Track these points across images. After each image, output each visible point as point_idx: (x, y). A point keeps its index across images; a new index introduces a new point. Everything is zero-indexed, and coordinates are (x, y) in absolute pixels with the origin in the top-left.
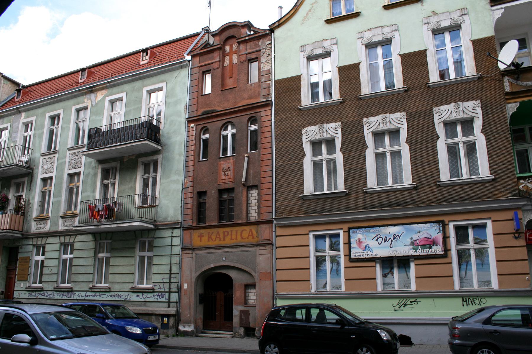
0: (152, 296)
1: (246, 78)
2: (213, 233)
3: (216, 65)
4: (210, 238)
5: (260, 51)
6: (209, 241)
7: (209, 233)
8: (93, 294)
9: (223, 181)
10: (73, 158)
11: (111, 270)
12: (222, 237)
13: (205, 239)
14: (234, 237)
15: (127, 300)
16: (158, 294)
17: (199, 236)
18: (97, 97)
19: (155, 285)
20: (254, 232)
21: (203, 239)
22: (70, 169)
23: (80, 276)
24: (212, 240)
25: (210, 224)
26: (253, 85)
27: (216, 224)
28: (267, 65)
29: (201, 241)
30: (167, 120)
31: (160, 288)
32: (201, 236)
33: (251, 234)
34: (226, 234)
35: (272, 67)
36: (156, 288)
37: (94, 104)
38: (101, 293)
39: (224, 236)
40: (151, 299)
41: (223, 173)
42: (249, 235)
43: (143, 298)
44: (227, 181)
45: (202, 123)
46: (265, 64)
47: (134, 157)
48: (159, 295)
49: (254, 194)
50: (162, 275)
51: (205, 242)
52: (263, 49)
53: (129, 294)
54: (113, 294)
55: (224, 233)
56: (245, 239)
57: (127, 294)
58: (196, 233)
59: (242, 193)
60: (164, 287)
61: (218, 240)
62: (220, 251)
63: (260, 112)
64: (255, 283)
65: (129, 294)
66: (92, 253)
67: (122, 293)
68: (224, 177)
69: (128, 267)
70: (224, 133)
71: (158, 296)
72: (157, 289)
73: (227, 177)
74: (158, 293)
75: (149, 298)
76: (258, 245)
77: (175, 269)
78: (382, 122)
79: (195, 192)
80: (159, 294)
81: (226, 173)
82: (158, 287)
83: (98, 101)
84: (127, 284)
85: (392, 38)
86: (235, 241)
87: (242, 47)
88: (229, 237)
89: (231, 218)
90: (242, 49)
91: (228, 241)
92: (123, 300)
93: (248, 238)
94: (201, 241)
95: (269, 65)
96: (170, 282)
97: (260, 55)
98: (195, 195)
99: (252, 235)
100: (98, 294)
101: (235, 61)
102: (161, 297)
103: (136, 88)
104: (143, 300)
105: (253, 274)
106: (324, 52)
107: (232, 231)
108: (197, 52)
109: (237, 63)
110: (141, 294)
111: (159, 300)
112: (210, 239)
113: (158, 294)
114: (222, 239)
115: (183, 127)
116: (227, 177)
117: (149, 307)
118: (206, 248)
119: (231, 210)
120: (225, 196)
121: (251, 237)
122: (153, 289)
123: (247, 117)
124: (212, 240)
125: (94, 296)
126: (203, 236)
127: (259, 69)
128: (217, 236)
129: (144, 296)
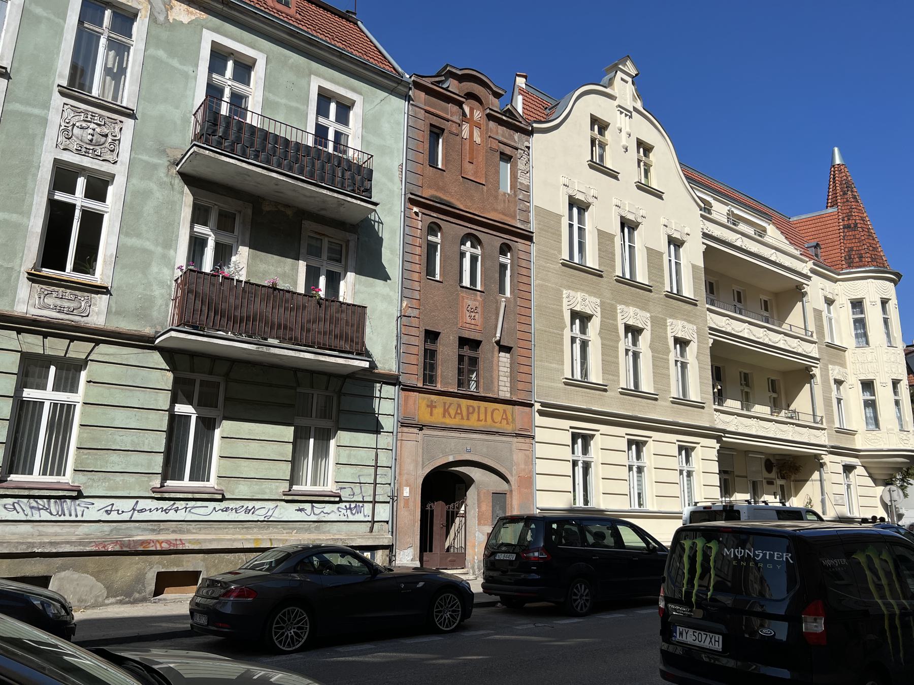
0: (336, 510)
2: (451, 404)
4: (446, 411)
5: (517, 149)
6: (444, 416)
7: (445, 403)
8: (166, 504)
9: (468, 325)
10: (84, 124)
12: (465, 413)
13: (438, 411)
14: (482, 417)
15: (270, 519)
16: (348, 507)
17: (428, 406)
19: (341, 488)
21: (435, 411)
22: (64, 149)
23: (114, 457)
24: (450, 416)
25: (445, 389)
29: (431, 415)
31: (353, 495)
32: (431, 406)
33: (504, 417)
36: (345, 495)
39: (468, 414)
40: (332, 517)
42: (502, 419)
44: (473, 327)
47: (289, 212)
48: (350, 508)
51: (437, 417)
53: (277, 506)
54: (232, 505)
56: (496, 423)
57: (271, 505)
59: (493, 352)
60: (361, 492)
62: (463, 435)
65: (277, 506)
67: (258, 505)
69: (275, 446)
71: (349, 511)
72: (347, 496)
74: (348, 505)
75: (328, 514)
76: (518, 435)
77: (384, 459)
80: (350, 505)
81: (473, 314)
83: (174, 19)
84: (274, 484)
86: (483, 423)
87: (492, 124)
88: (475, 415)
91: (473, 423)
93: (501, 423)
94: (431, 415)
96: (375, 484)
99: (506, 419)
100: (181, 505)
102: (354, 512)
104: (314, 518)
105: (509, 477)
107: (479, 407)
108: (427, 82)
110: (307, 506)
111: (351, 518)
112: (447, 413)
113: (348, 507)
114: (465, 417)
117: (329, 532)
121: (504, 422)
124: (450, 416)
125: (166, 511)
126: (435, 407)
128: (457, 410)
129: (317, 511)
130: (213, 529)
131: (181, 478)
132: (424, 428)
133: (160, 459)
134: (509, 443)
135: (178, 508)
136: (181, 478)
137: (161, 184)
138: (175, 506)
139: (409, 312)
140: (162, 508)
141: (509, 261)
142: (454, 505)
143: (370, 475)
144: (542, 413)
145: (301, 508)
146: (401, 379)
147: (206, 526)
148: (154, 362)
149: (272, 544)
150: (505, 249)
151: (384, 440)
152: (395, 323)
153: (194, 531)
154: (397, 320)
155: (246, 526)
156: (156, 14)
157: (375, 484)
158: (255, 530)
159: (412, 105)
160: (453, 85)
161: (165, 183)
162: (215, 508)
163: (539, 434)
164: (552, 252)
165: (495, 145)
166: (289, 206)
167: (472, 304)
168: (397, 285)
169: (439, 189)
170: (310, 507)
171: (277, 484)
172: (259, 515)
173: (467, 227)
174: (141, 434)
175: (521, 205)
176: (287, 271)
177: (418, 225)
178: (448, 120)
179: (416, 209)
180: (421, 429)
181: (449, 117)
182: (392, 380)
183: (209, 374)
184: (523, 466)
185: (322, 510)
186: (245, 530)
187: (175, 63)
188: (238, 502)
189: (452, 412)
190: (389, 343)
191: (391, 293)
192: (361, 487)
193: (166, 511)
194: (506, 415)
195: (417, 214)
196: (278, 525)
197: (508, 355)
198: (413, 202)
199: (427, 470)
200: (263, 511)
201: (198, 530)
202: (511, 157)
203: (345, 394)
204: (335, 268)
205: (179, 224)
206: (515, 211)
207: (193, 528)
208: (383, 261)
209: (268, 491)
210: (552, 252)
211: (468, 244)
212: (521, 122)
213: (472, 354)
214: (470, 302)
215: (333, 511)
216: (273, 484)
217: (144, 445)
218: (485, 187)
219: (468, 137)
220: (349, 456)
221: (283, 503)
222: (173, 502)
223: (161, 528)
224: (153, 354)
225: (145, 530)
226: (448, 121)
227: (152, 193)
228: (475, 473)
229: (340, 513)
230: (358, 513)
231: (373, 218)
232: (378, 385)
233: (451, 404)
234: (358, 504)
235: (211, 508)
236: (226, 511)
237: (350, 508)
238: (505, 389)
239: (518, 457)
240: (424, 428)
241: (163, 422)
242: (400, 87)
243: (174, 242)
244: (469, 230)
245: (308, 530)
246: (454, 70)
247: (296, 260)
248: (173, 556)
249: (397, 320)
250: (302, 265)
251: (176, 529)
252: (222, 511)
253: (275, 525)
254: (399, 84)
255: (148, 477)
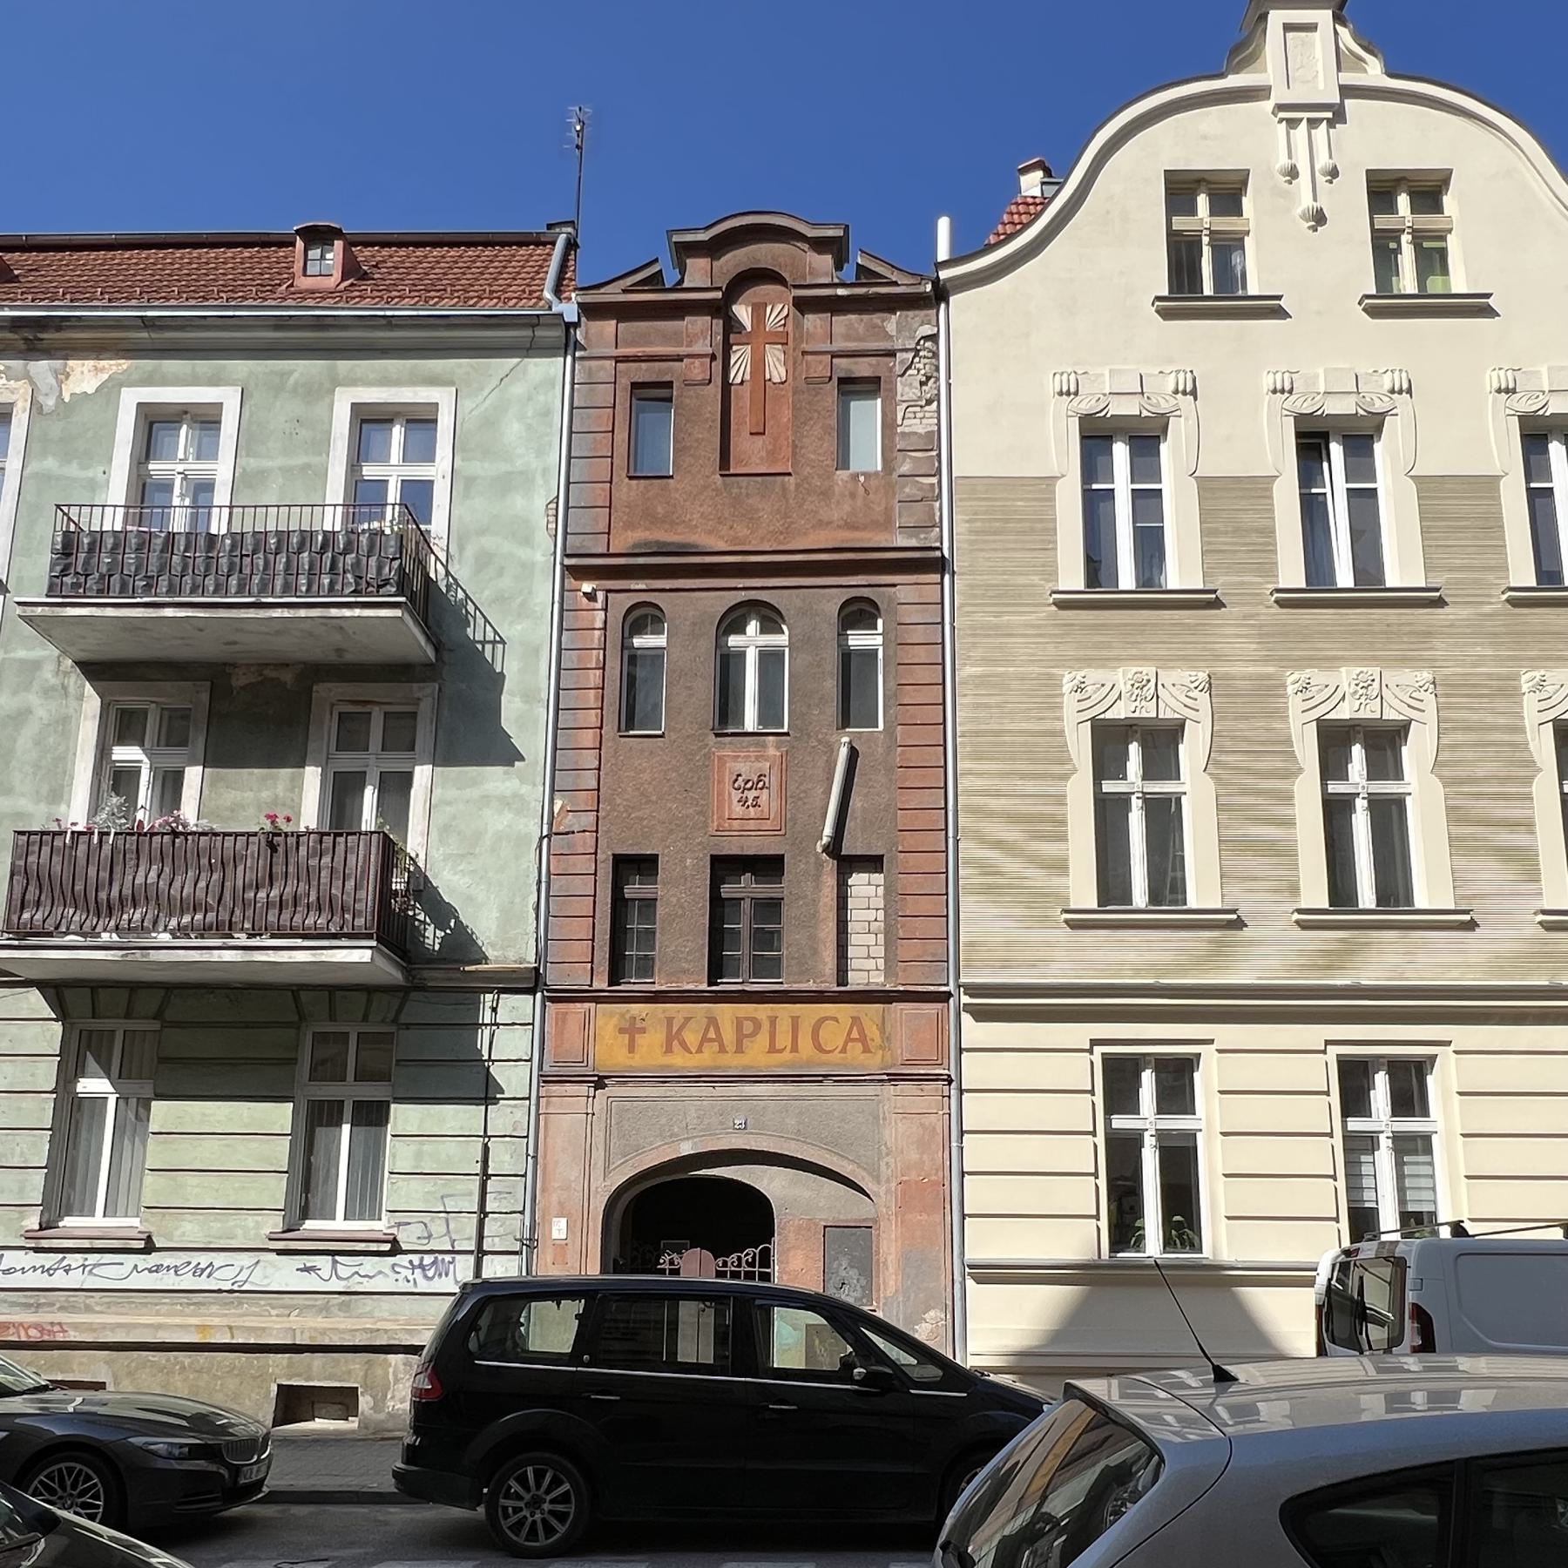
0: (387, 1271)
1: (831, 444)
2: (688, 1020)
3: (697, 370)
4: (673, 1039)
5: (891, 354)
6: (669, 1050)
7: (670, 1021)
8: (49, 1260)
11: (156, 1153)
12: (729, 1035)
13: (652, 1040)
14: (784, 1040)
15: (243, 1288)
16: (416, 1263)
18: (68, 376)
19: (399, 1224)
20: (873, 1032)
21: (641, 1040)
25: (673, 986)
26: (862, 479)
27: (704, 987)
28: (919, 415)
29: (632, 1048)
30: (461, 548)
31: (430, 1237)
33: (855, 1034)
34: (748, 1027)
35: (939, 425)
36: (407, 1239)
37: (50, 403)
38: (93, 1258)
39: (740, 1038)
41: (736, 795)
42: (849, 1039)
43: (338, 1278)
44: (752, 825)
45: (633, 587)
46: (910, 409)
47: (287, 677)
48: (421, 1266)
49: (863, 886)
50: (440, 1180)
51: (651, 1052)
52: (906, 350)
53: (258, 1262)
54: (167, 1259)
55: (739, 1023)
56: (829, 1052)
57: (246, 1259)
58: (608, 1017)
59: (817, 878)
60: (448, 1231)
61: (710, 1050)
62: (721, 1090)
63: (894, 585)
64: (875, 1221)
65: (258, 1262)
66: (46, 1074)
67: (219, 1259)
68: (738, 810)
69: (254, 1144)
70: (734, 641)
71: (418, 1271)
72: (416, 1240)
73: (752, 812)
74: (416, 1258)
75: (371, 1277)
76: (895, 1078)
77: (504, 1158)
78: (1356, 692)
79: (605, 856)
81: (751, 794)
82: (417, 1230)
84: (251, 1220)
85: (1383, 415)
87: (813, 321)
88: (763, 1039)
89: (771, 967)
90: (811, 330)
91: (757, 1056)
92: (228, 1287)
93: (844, 1051)
94: (632, 1048)
95: (927, 415)
96: (483, 1213)
97: (891, 370)
98: (606, 871)
99: (863, 1039)
100: (75, 1260)
101: (776, 369)
102: (430, 1274)
103: (292, 380)
106: (1145, 413)
107: (773, 1021)
108: (612, 294)
109: (783, 383)
110: (324, 1262)
111: (423, 1286)
113: (416, 1263)
115: (544, 591)
116: (752, 812)
117: (370, 1315)
118: (664, 1080)
119: (767, 939)
120: (745, 887)
122: (395, 1242)
123: (836, 599)
125: (49, 1271)
126: (643, 1030)
127: (889, 425)
128: (707, 1030)
130: (133, 1305)
131: (92, 1214)
132: (606, 1081)
133: (38, 1178)
134: (867, 1098)
135: (70, 1265)
136: (92, 1214)
137: (47, 692)
138: (64, 1263)
139: (570, 822)
140: (43, 1267)
141: (879, 640)
142: (739, 1259)
143: (471, 1194)
144: (981, 1015)
145: (308, 1265)
146: (554, 977)
147: (120, 1300)
148: (28, 1009)
149: (233, 1337)
150: (859, 613)
151: (504, 1117)
152: (532, 855)
153: (97, 1308)
154: (540, 847)
155: (194, 1300)
156: (41, 399)
157: (483, 1213)
158: (214, 1309)
159: (582, 358)
160: (698, 272)
161: (53, 688)
162: (136, 1266)
163: (974, 1070)
164: (1021, 580)
165: (820, 367)
166: (287, 665)
167: (747, 769)
168: (540, 768)
169: (652, 519)
170: (330, 1262)
171: (259, 1218)
172: (224, 1279)
173: (736, 589)
174: (10, 1137)
175: (907, 490)
176: (281, 794)
177: (593, 620)
178: (679, 359)
179: (587, 587)
180: (600, 1083)
181: (682, 350)
182: (529, 982)
183: (125, 1018)
184: (914, 1156)
185: (356, 1269)
186: (192, 1307)
187: (73, 470)
188: (181, 1254)
189: (691, 1038)
190: (518, 900)
191: (525, 789)
192: (447, 1220)
193: (49, 1271)
194: (862, 1032)
195: (591, 597)
196: (261, 1299)
197: (878, 878)
198: (579, 573)
199: (620, 1179)
200: (228, 1272)
201: (105, 1306)
202: (876, 380)
203: (408, 1026)
204: (394, 763)
205: (75, 754)
206: (888, 512)
207: (97, 1304)
208: (504, 724)
209: (239, 1232)
210: (1021, 580)
211: (753, 627)
212: (895, 284)
213: (764, 890)
214: (743, 768)
215: (380, 1272)
216: (250, 1218)
217: (13, 1155)
218: (792, 479)
219: (747, 377)
220: (419, 1156)
221: (273, 1256)
222: (61, 1256)
223: (43, 1301)
224: (28, 995)
225: (13, 1304)
226: (682, 360)
227: (31, 712)
228: (768, 1181)
229: (397, 1276)
230: (440, 1275)
231: (479, 637)
232: (489, 997)
233: (688, 1020)
234: (440, 1257)
235: (128, 1267)
236: (156, 1271)
237: (421, 1266)
238: (870, 964)
239: (896, 1133)
240: (606, 1081)
241: (42, 1111)
242: (539, 333)
243: (66, 789)
244: (743, 593)
245: (325, 1310)
246: (689, 238)
247: (300, 767)
248: (55, 1352)
249: (540, 847)
250: (313, 776)
251: (66, 1305)
252: (150, 1271)
253: (253, 1299)
254: (533, 326)
255: (21, 1212)
